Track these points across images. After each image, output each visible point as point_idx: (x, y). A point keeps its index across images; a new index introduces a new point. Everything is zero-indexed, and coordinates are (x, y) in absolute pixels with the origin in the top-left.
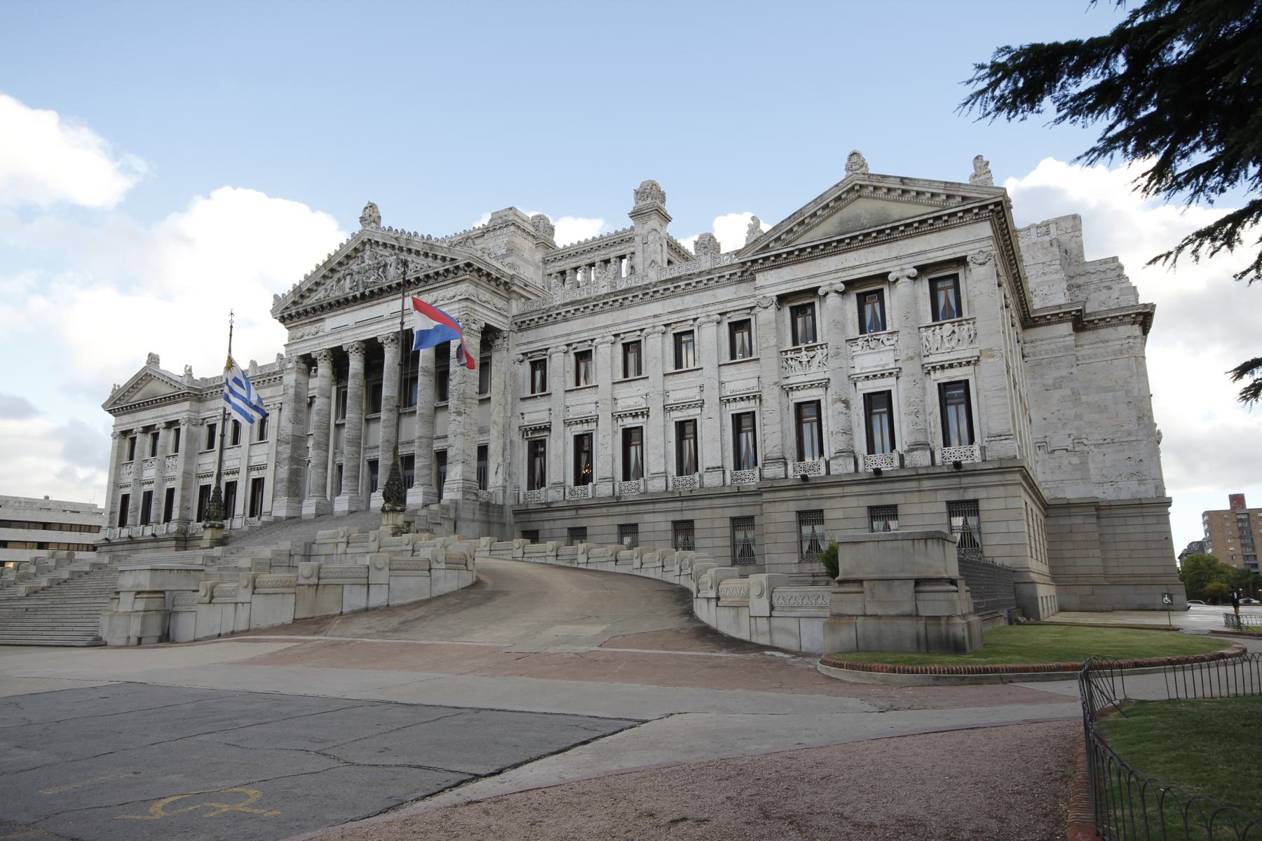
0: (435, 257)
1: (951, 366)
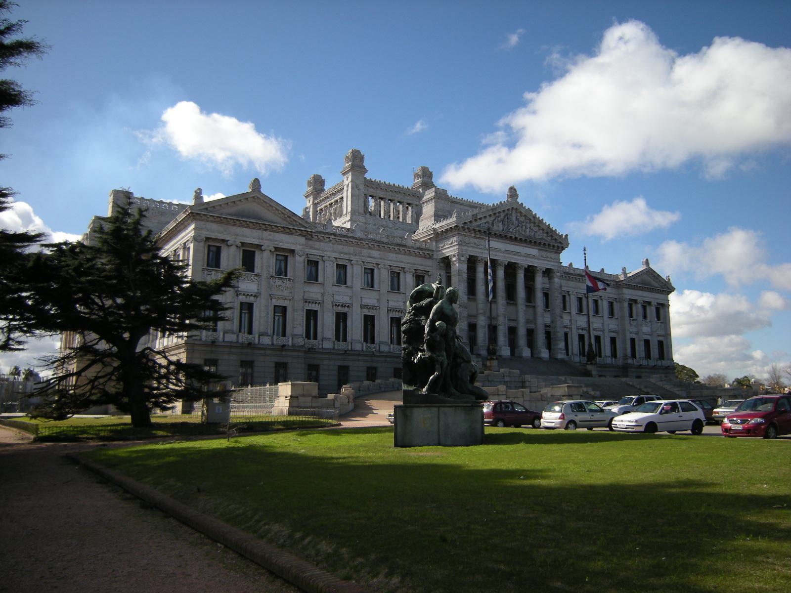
0: (552, 236)
1: (661, 336)
